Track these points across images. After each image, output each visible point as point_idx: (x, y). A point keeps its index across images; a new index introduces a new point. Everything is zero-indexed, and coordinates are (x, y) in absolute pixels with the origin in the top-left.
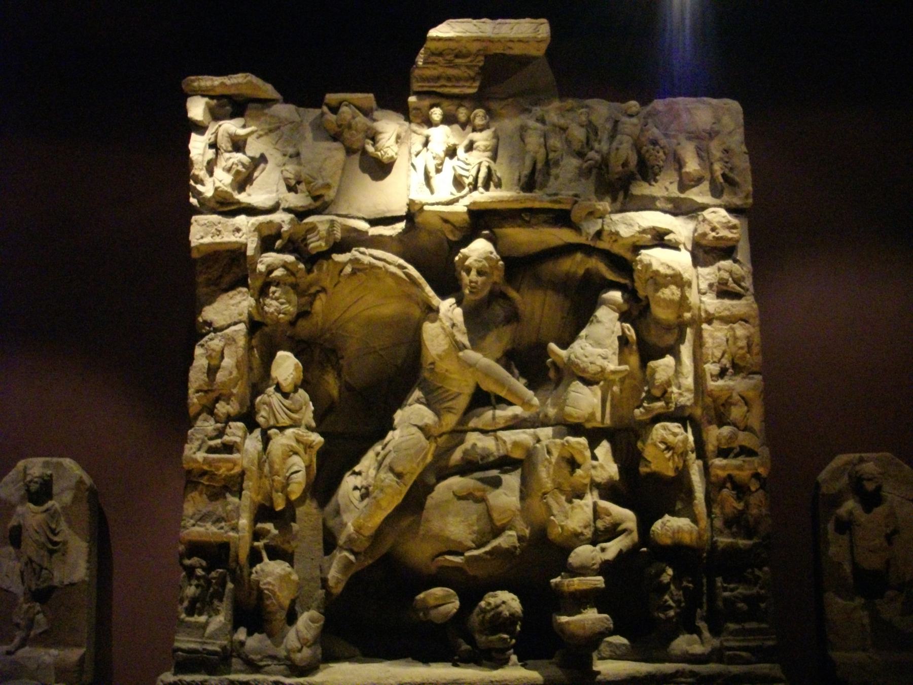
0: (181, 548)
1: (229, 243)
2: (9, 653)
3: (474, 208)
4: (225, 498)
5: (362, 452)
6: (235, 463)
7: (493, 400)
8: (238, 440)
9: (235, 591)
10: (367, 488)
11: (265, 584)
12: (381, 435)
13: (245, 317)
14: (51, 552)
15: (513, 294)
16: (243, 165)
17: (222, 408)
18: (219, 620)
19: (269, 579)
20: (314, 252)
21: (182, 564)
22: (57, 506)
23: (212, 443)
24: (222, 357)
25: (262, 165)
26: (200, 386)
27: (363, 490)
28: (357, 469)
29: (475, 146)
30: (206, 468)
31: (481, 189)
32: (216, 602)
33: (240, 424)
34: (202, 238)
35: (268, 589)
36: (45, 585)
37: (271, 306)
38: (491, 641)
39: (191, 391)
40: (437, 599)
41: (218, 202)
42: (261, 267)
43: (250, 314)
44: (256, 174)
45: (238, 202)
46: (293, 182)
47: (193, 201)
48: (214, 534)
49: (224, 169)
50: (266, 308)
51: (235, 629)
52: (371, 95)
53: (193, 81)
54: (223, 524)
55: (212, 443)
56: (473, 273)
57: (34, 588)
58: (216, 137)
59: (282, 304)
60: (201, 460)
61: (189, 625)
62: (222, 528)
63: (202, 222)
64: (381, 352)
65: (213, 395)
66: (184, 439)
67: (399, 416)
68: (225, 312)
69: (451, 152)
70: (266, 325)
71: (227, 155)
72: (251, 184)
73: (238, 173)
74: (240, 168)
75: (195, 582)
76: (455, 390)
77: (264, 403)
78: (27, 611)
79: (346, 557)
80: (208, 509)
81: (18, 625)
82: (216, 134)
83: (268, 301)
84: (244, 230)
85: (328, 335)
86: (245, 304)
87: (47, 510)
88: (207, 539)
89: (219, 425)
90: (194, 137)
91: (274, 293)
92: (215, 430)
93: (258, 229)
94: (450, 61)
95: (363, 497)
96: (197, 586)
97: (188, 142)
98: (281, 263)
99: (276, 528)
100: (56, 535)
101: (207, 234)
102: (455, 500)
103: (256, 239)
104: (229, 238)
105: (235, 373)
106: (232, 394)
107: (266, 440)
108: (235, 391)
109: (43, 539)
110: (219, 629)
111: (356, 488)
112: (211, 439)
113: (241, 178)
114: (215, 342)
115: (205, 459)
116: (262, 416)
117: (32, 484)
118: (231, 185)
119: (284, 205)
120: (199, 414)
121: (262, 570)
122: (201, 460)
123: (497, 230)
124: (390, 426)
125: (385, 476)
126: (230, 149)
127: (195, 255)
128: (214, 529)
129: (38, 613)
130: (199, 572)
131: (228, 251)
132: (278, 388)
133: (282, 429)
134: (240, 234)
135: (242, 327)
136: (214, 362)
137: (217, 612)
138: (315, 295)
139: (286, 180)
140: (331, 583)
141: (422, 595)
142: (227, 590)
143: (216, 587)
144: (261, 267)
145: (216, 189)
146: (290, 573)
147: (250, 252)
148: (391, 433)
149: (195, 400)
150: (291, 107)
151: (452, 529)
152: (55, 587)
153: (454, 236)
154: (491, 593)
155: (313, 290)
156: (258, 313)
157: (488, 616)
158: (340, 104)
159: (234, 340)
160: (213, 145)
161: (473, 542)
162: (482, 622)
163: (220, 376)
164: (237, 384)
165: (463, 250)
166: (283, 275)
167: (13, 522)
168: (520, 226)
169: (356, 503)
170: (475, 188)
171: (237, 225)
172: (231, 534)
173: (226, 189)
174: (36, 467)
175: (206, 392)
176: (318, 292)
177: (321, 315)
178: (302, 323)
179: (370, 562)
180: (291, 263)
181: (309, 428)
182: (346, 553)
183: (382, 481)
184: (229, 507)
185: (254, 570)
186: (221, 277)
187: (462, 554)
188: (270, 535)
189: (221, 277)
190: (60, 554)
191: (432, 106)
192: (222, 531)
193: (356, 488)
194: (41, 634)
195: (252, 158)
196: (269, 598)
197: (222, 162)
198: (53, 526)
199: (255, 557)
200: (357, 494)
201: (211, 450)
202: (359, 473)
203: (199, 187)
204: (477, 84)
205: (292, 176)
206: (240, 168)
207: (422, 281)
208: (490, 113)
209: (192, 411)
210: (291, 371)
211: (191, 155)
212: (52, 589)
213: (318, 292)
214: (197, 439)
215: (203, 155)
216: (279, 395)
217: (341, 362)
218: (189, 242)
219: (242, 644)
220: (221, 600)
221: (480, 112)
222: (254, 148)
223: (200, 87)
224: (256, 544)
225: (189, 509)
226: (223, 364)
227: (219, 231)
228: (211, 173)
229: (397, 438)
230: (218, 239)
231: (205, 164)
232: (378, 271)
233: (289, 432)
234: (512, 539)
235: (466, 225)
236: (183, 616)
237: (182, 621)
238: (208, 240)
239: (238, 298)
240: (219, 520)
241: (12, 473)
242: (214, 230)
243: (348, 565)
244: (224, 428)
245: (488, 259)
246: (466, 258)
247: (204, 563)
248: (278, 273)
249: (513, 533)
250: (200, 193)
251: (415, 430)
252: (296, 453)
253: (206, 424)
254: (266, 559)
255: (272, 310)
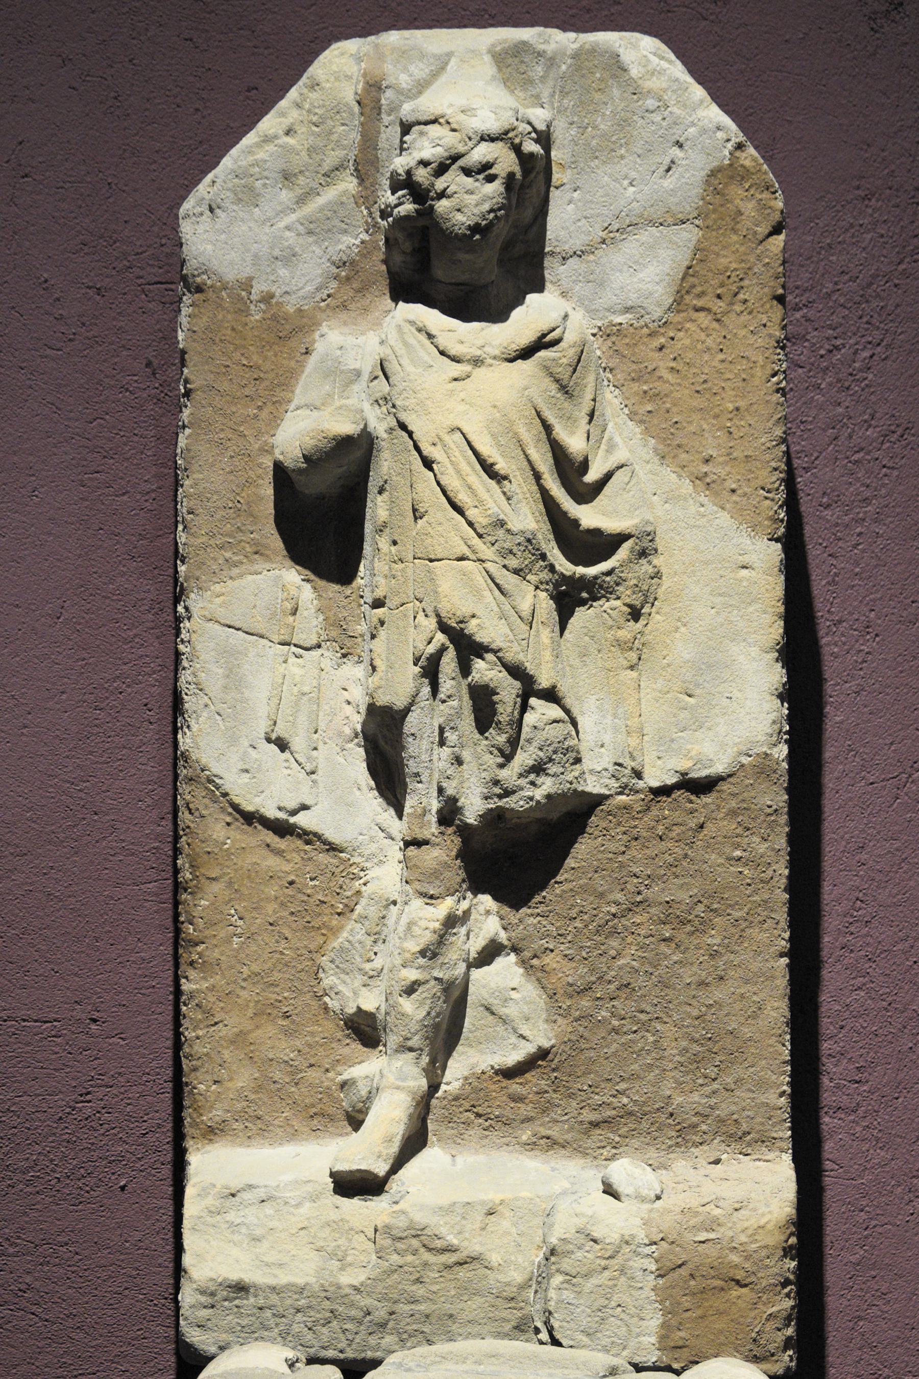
2: (355, 1185)
14: (569, 598)
22: (578, 328)
36: (547, 786)
57: (473, 808)
78: (431, 953)
81: (365, 1030)
87: (541, 344)
100: (586, 494)
109: (528, 519)
117: (453, 180)
129: (490, 953)
152: (597, 801)
167: (297, 432)
174: (461, 89)
190: (613, 606)
194: (509, 1073)
198: (575, 444)
212: (572, 816)
241: (278, 132)
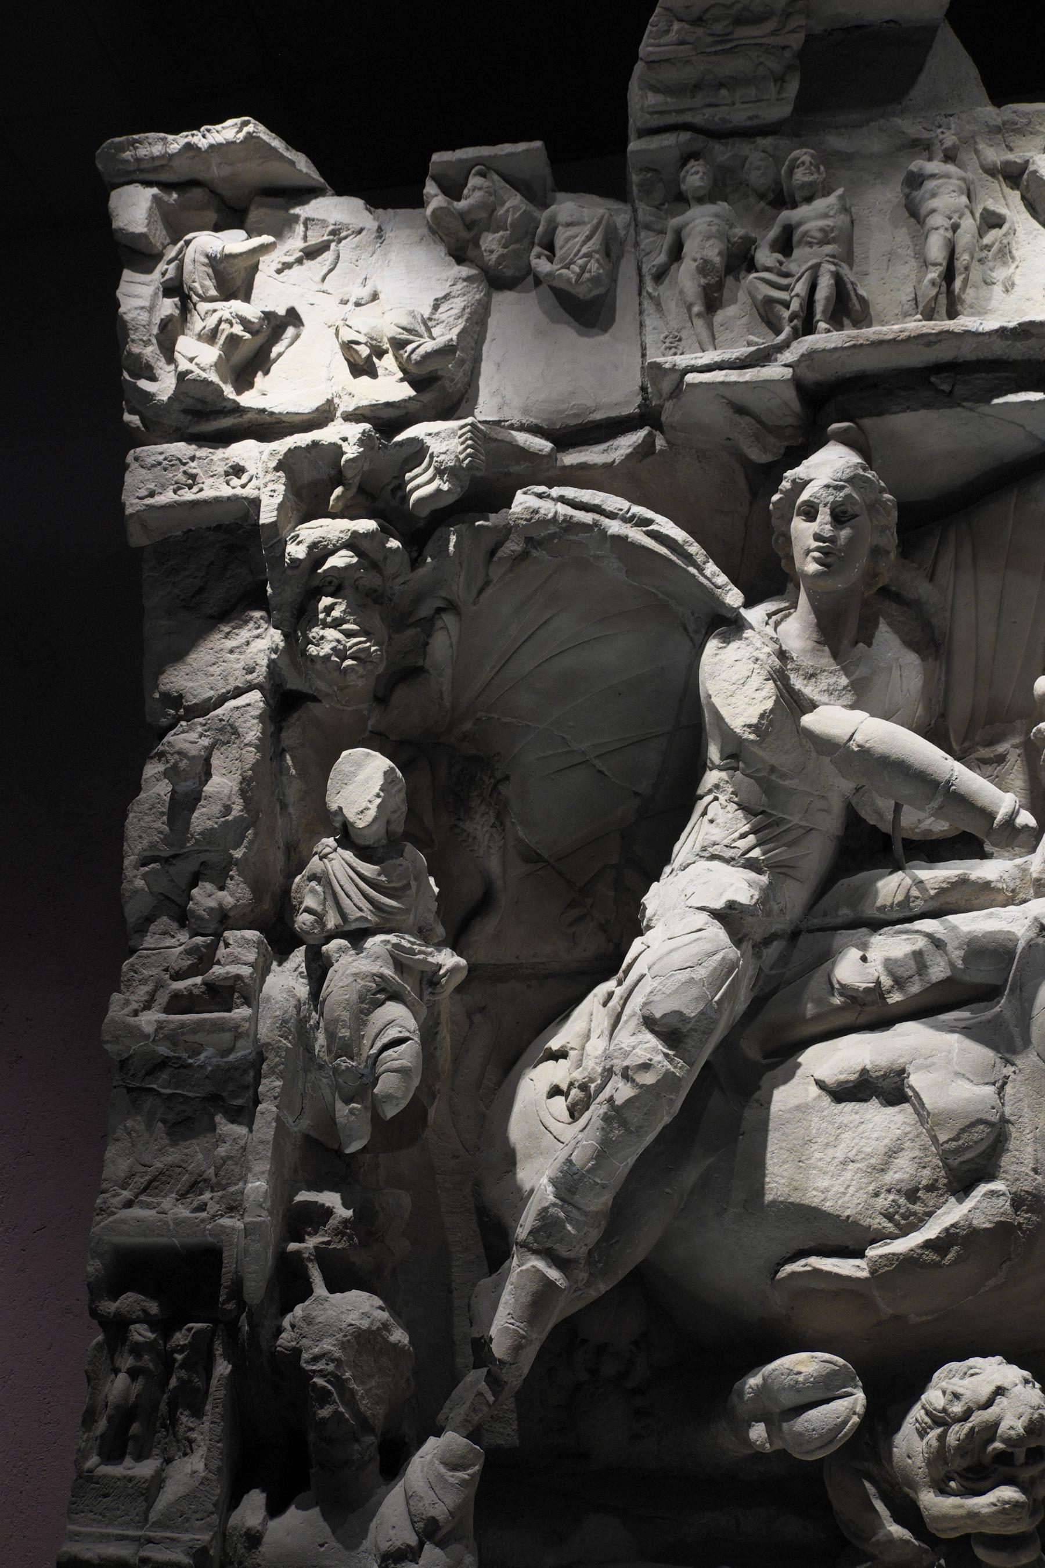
0: (94, 1267)
1: (217, 500)
3: (811, 376)
4: (213, 1127)
5: (562, 1012)
6: (236, 1032)
7: (898, 848)
8: (246, 971)
9: (234, 1380)
10: (584, 1087)
11: (316, 1359)
12: (609, 963)
13: (260, 675)
15: (922, 589)
16: (244, 322)
17: (205, 897)
18: (192, 1469)
19: (327, 1345)
20: (424, 513)
21: (94, 1313)
23: (180, 985)
24: (208, 775)
25: (290, 331)
26: (153, 846)
27: (574, 1092)
28: (555, 1044)
29: (796, 238)
30: (163, 1050)
31: (822, 325)
32: (185, 1419)
33: (252, 934)
34: (152, 494)
35: (322, 1374)
37: (326, 640)
38: (973, 1515)
39: (129, 861)
40: (795, 1388)
41: (186, 411)
42: (296, 551)
43: (272, 665)
44: (276, 350)
45: (238, 409)
46: (364, 351)
47: (132, 419)
48: (179, 1222)
49: (200, 337)
50: (312, 650)
51: (234, 1500)
52: (538, 144)
53: (122, 148)
54: (207, 1196)
55: (180, 985)
56: (824, 516)
58: (180, 269)
59: (349, 634)
60: (149, 1029)
61: (106, 1488)
62: (202, 1207)
63: (150, 460)
64: (599, 764)
65: (185, 868)
66: (114, 982)
67: (656, 898)
68: (212, 669)
69: (740, 260)
70: (315, 699)
71: (203, 307)
72: (266, 373)
73: (233, 340)
74: (238, 329)
75: (127, 1362)
76: (795, 819)
77: (313, 877)
79: (538, 1271)
80: (169, 1159)
82: (179, 259)
83: (316, 632)
84: (252, 469)
85: (468, 726)
86: (263, 644)
88: (164, 1240)
89: (199, 940)
90: (127, 274)
91: (329, 609)
92: (188, 952)
93: (286, 464)
94: (724, 38)
95: (574, 1112)
96: (134, 1374)
97: (117, 285)
98: (346, 537)
99: (346, 1206)
101: (164, 487)
102: (827, 1100)
103: (281, 488)
104: (215, 488)
105: (237, 810)
106: (231, 862)
107: (318, 970)
108: (238, 854)
110: (190, 1497)
111: (555, 1091)
112: (178, 976)
113: (241, 354)
114: (188, 739)
115: (160, 1025)
116: (309, 911)
118: (217, 366)
119: (346, 405)
120: (150, 919)
121: (308, 1320)
122: (149, 1029)
123: (867, 422)
124: (633, 925)
125: (633, 1041)
126: (213, 292)
127: (137, 538)
128: (184, 1212)
130: (141, 1333)
131: (219, 528)
132: (347, 837)
133: (357, 937)
134: (245, 478)
135: (255, 696)
136: (185, 786)
137: (188, 1447)
138: (428, 625)
139: (348, 347)
140: (499, 1349)
141: (754, 1381)
142: (214, 1382)
143: (183, 1373)
144: (296, 551)
145: (181, 376)
146: (385, 1326)
147: (267, 516)
148: (637, 945)
149: (140, 883)
150: (358, 203)
151: (824, 1183)
153: (765, 449)
154: (954, 1365)
155: (425, 611)
156: (294, 663)
157: (956, 1433)
158: (466, 168)
159: (235, 732)
160: (175, 288)
161: (889, 1217)
162: (939, 1456)
163: (202, 819)
164: (244, 837)
165: (789, 473)
166: (348, 567)
168: (927, 406)
169: (556, 1127)
170: (808, 327)
171: (237, 460)
172: (226, 1221)
173: (204, 375)
175: (167, 861)
176: (439, 610)
177: (449, 671)
178: (401, 695)
179: (603, 1287)
180: (369, 535)
181: (423, 934)
182: (540, 1264)
183: (626, 1054)
184: (222, 1151)
185: (286, 1322)
186: (201, 590)
187: (860, 1254)
188: (333, 1222)
189: (201, 590)
191: (689, 156)
192: (204, 1215)
193: (555, 1091)
195: (268, 316)
196: (324, 1397)
197: (197, 325)
199: (289, 1283)
200: (560, 1101)
201: (179, 1004)
202: (561, 1055)
203: (144, 384)
204: (793, 87)
205: (362, 339)
206: (238, 329)
207: (695, 549)
208: (828, 159)
209: (133, 911)
210: (377, 790)
211: (121, 310)
213: (439, 610)
214: (144, 981)
215: (151, 309)
216: (348, 855)
217: (504, 789)
218: (122, 507)
219: (254, 1539)
220: (198, 1413)
221: (804, 155)
222: (271, 293)
223: (138, 160)
224: (293, 1246)
225: (118, 1161)
226: (208, 789)
227: (193, 477)
228: (169, 352)
229: (655, 945)
230: (188, 495)
231: (155, 331)
232: (582, 536)
233: (374, 942)
234: (1001, 1201)
235: (791, 421)
236: (94, 1460)
237: (87, 1478)
238: (167, 497)
239: (245, 634)
240: (195, 1186)
242: (180, 477)
243: (543, 1294)
244: (213, 947)
245: (852, 480)
246: (800, 485)
247: (153, 1308)
248: (341, 560)
249: (998, 1186)
250: (149, 396)
251: (704, 916)
252: (396, 996)
253: (169, 942)
254: (320, 1289)
255: (326, 649)
